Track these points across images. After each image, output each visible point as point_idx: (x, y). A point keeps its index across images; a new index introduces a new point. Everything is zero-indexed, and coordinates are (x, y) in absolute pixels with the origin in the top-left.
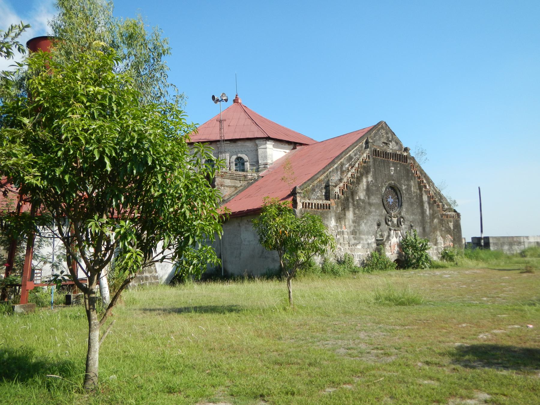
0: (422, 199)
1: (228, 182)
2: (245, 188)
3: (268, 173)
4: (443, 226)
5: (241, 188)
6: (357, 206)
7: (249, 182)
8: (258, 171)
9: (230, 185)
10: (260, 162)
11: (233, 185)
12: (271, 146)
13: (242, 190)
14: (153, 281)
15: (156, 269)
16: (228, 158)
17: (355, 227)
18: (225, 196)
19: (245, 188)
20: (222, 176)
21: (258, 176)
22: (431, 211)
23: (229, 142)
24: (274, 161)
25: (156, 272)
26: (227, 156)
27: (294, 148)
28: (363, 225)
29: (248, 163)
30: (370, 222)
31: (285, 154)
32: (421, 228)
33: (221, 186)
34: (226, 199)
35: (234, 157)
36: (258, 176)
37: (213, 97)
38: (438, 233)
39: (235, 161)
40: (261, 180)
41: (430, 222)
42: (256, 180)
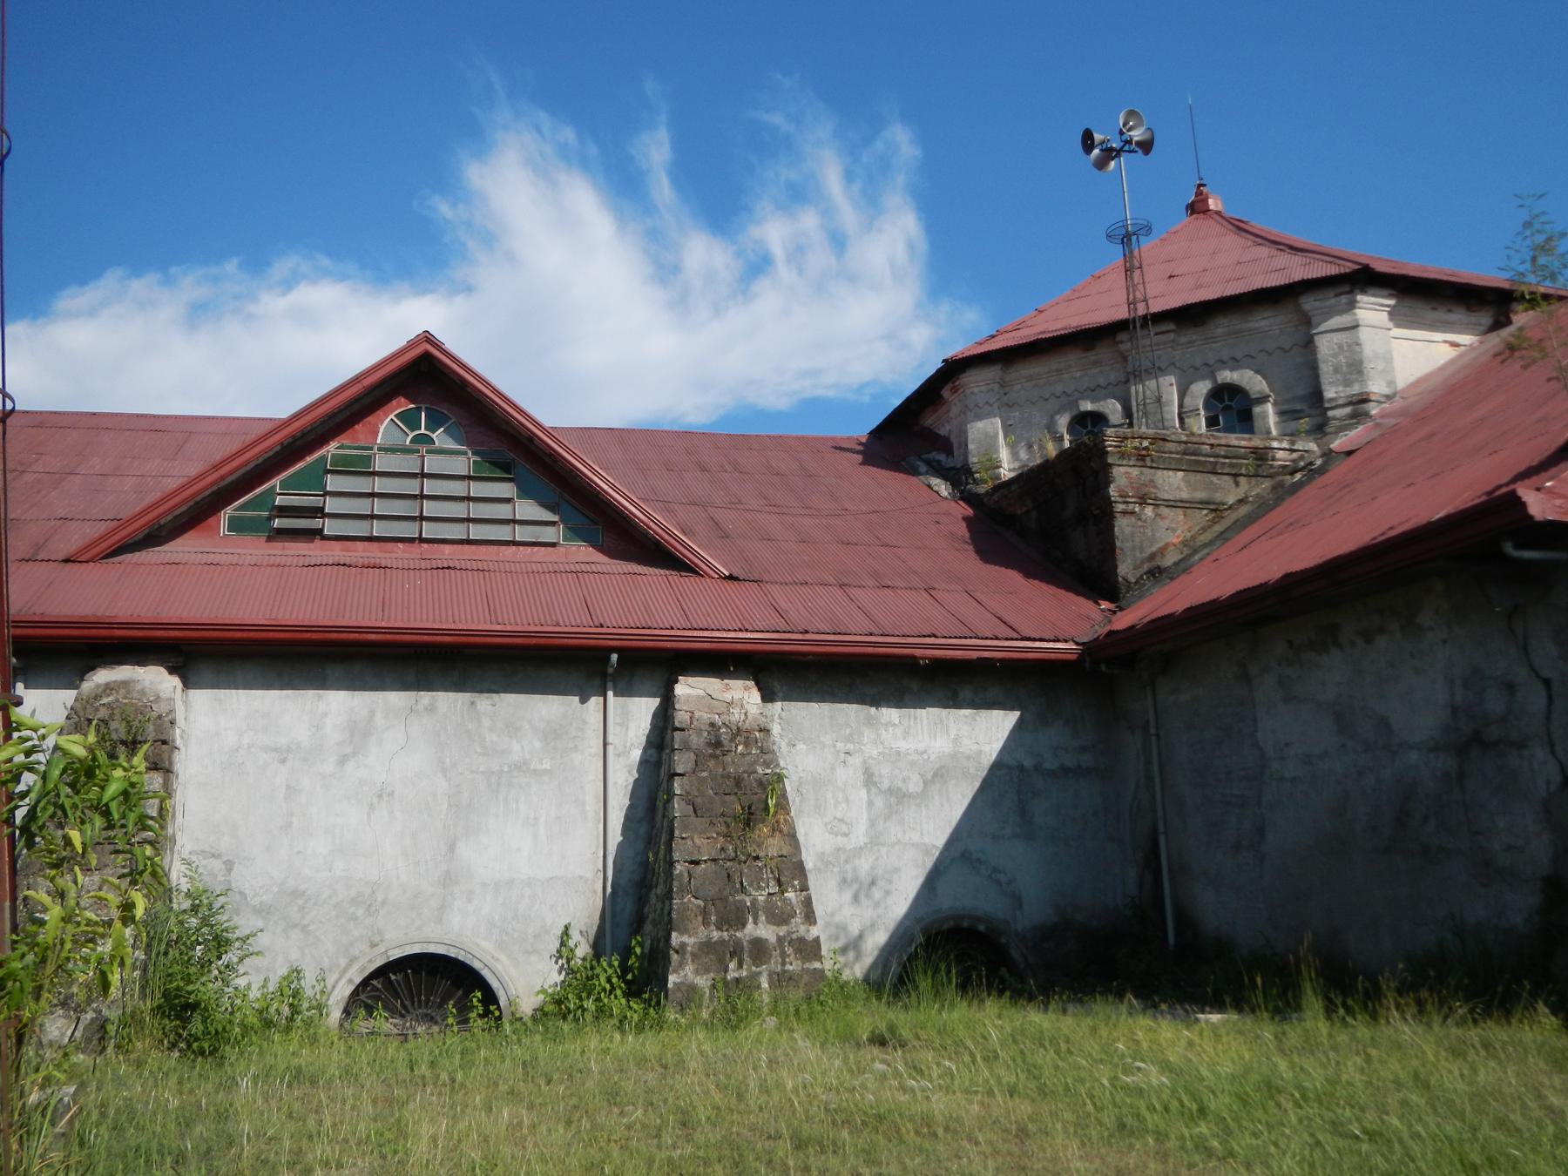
1: (1173, 483)
2: (1263, 508)
3: (1377, 433)
5: (1243, 510)
7: (1281, 484)
8: (1320, 429)
9: (1185, 495)
10: (1330, 393)
11: (1200, 495)
12: (1382, 317)
13: (1250, 520)
14: (794, 966)
15: (808, 903)
16: (1175, 399)
18: (1162, 551)
19: (1263, 508)
20: (1142, 458)
21: (1328, 455)
23: (1172, 326)
24: (1401, 384)
25: (810, 918)
26: (1169, 387)
27: (1500, 323)
29: (1269, 408)
31: (1451, 353)
33: (1143, 500)
34: (1169, 560)
35: (1202, 388)
36: (1328, 455)
37: (1088, 141)
39: (1207, 406)
40: (1340, 470)
42: (1312, 472)
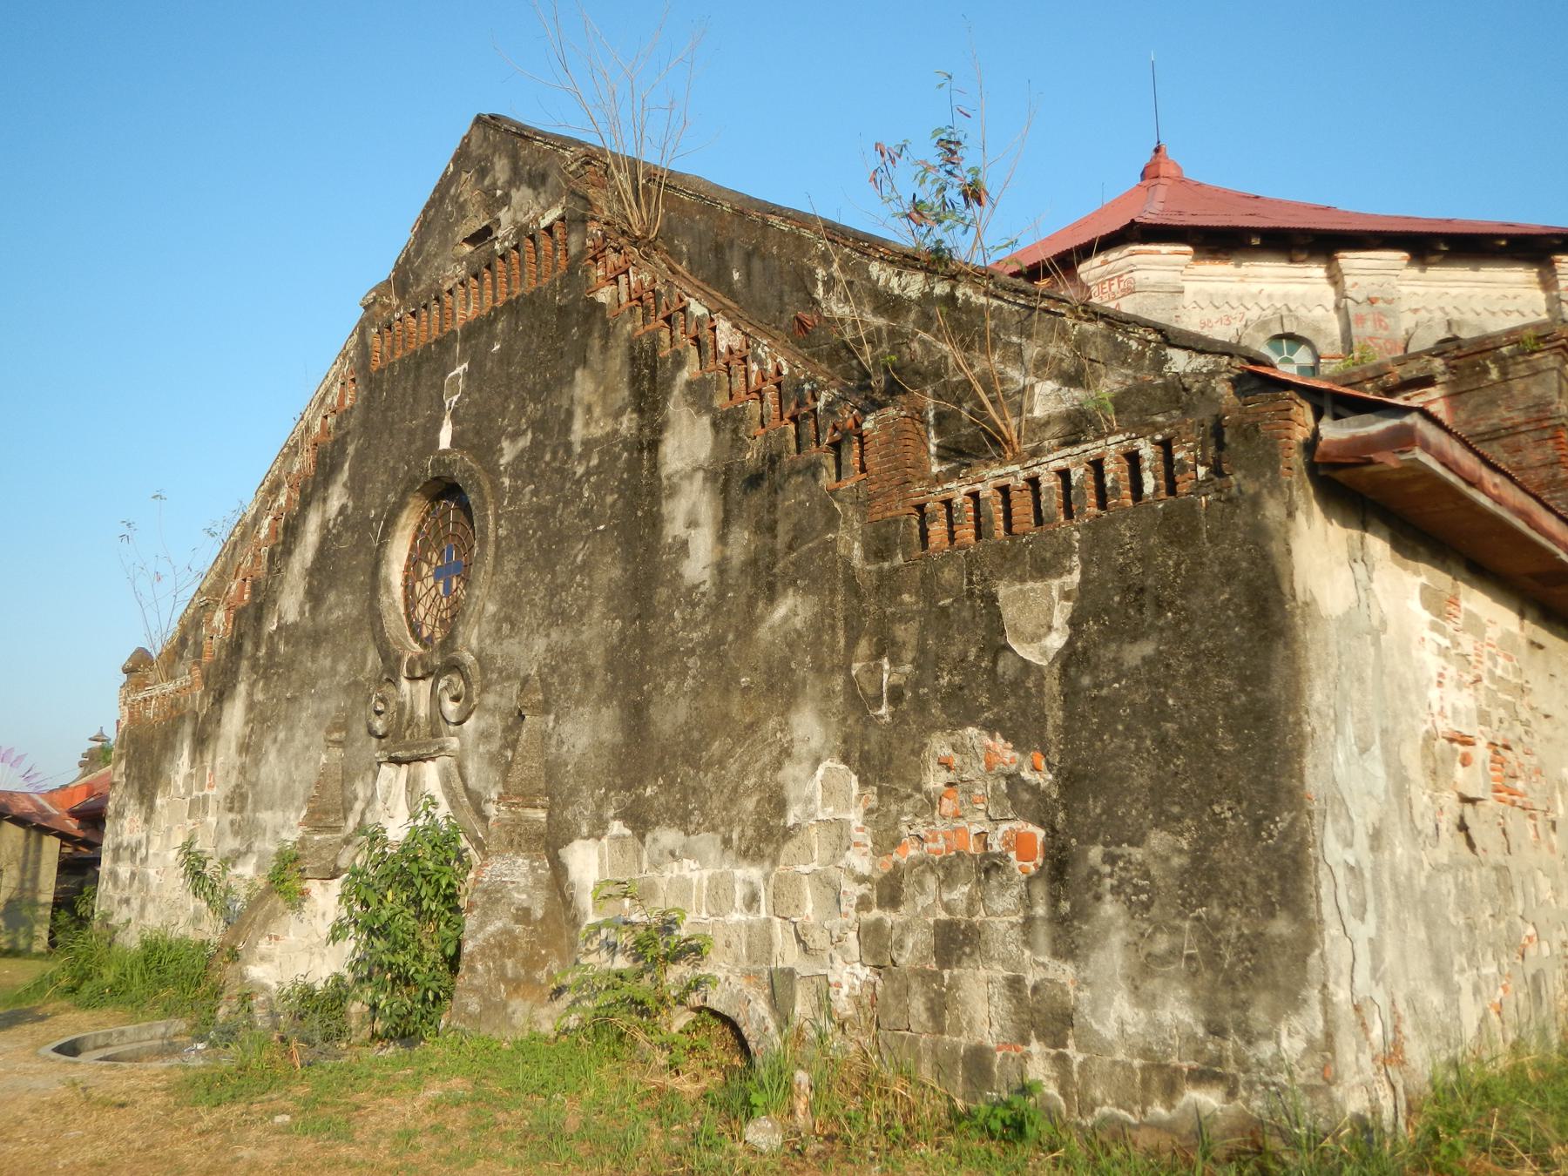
0: (655, 467)
4: (885, 646)
6: (266, 671)
17: (243, 770)
22: (742, 539)
28: (272, 756)
30: (299, 734)
32: (609, 714)
38: (808, 727)
41: (713, 646)
